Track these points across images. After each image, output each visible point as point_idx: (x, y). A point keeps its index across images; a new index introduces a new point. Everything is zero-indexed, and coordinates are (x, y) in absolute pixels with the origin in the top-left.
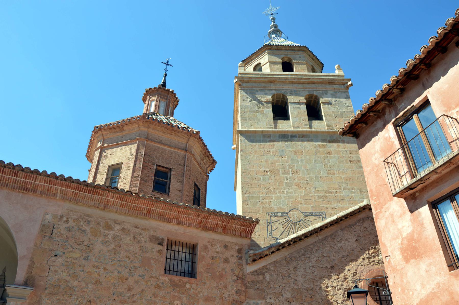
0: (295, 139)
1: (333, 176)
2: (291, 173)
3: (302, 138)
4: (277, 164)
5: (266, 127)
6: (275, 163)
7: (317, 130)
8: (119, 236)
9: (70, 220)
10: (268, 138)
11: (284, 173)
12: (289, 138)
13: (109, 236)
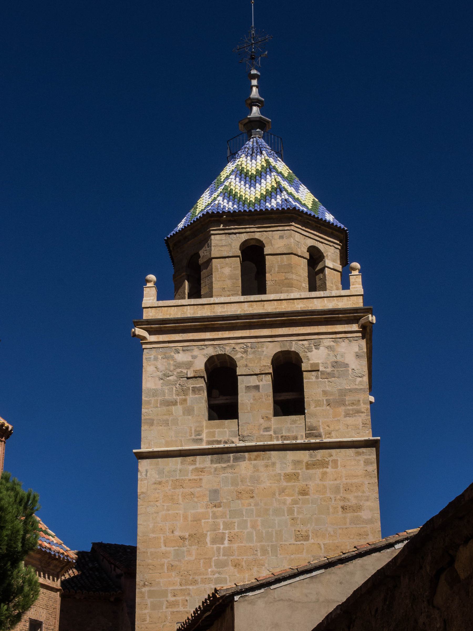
0: (241, 463)
1: (304, 543)
2: (227, 539)
3: (255, 460)
4: (203, 521)
5: (189, 439)
6: (200, 520)
7: (286, 442)
10: (192, 464)
11: (214, 541)
12: (230, 462)
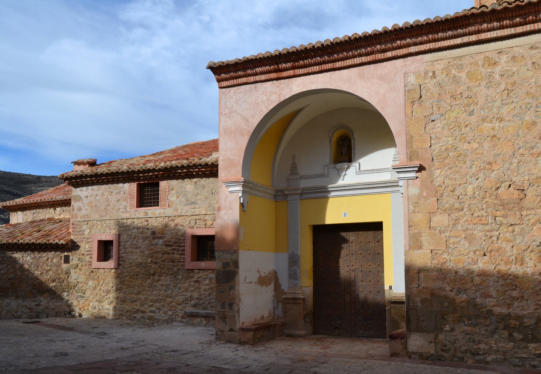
8: (509, 70)
9: (437, 73)
13: (494, 75)
